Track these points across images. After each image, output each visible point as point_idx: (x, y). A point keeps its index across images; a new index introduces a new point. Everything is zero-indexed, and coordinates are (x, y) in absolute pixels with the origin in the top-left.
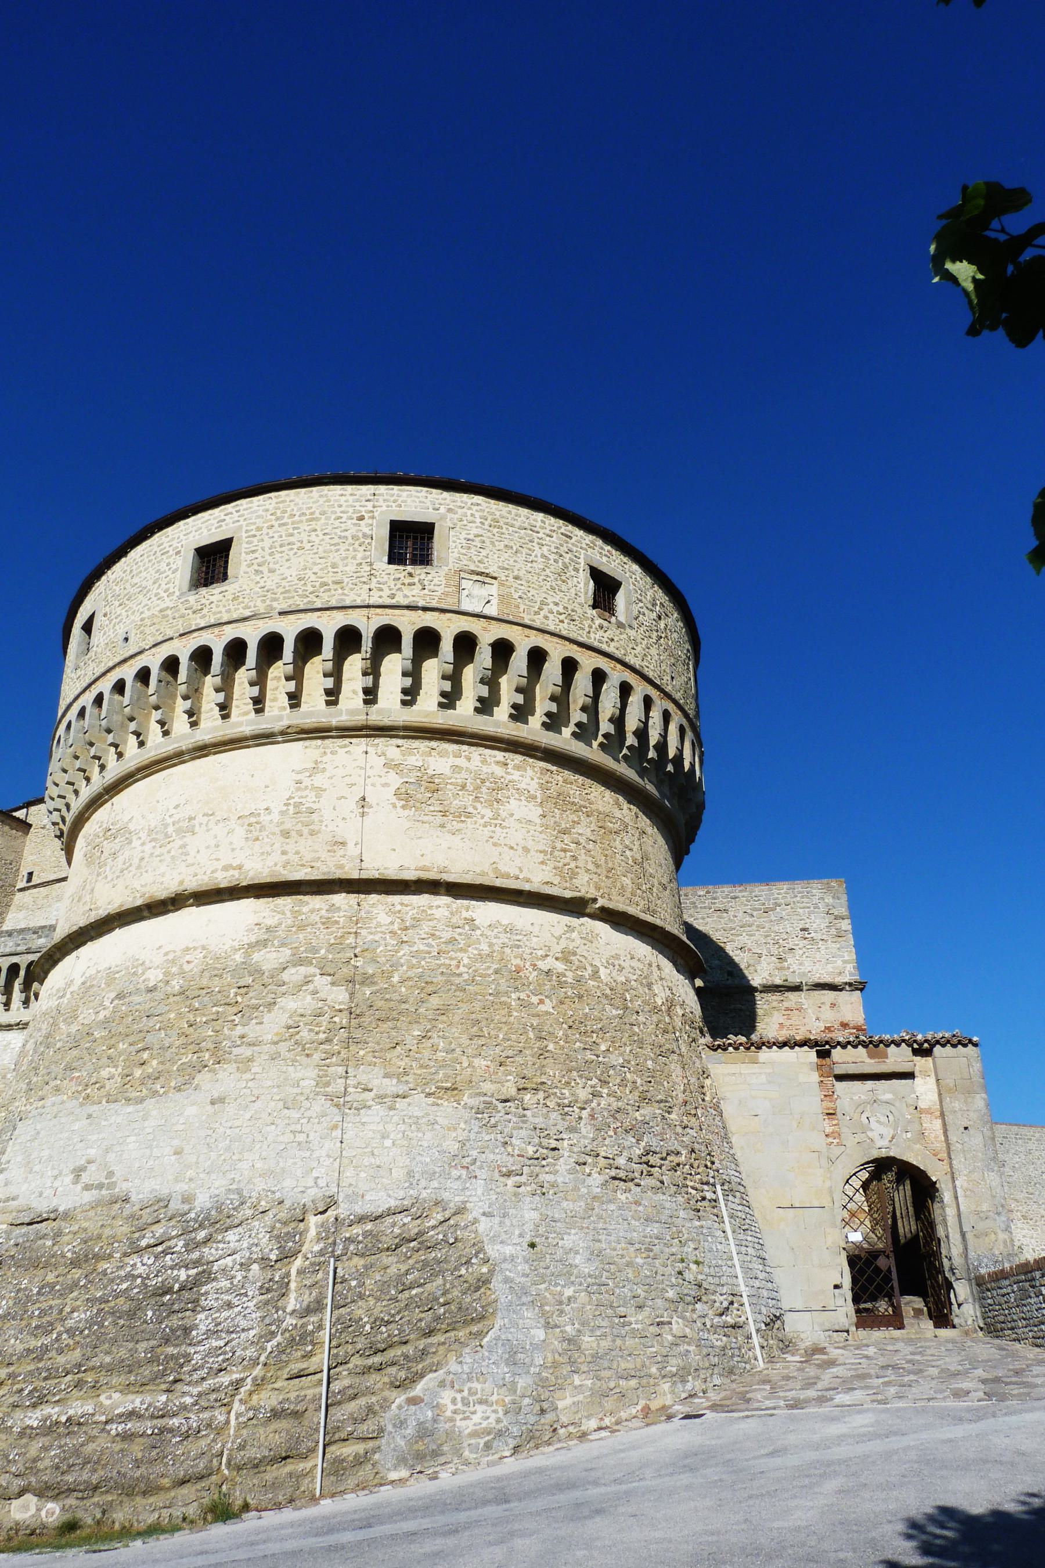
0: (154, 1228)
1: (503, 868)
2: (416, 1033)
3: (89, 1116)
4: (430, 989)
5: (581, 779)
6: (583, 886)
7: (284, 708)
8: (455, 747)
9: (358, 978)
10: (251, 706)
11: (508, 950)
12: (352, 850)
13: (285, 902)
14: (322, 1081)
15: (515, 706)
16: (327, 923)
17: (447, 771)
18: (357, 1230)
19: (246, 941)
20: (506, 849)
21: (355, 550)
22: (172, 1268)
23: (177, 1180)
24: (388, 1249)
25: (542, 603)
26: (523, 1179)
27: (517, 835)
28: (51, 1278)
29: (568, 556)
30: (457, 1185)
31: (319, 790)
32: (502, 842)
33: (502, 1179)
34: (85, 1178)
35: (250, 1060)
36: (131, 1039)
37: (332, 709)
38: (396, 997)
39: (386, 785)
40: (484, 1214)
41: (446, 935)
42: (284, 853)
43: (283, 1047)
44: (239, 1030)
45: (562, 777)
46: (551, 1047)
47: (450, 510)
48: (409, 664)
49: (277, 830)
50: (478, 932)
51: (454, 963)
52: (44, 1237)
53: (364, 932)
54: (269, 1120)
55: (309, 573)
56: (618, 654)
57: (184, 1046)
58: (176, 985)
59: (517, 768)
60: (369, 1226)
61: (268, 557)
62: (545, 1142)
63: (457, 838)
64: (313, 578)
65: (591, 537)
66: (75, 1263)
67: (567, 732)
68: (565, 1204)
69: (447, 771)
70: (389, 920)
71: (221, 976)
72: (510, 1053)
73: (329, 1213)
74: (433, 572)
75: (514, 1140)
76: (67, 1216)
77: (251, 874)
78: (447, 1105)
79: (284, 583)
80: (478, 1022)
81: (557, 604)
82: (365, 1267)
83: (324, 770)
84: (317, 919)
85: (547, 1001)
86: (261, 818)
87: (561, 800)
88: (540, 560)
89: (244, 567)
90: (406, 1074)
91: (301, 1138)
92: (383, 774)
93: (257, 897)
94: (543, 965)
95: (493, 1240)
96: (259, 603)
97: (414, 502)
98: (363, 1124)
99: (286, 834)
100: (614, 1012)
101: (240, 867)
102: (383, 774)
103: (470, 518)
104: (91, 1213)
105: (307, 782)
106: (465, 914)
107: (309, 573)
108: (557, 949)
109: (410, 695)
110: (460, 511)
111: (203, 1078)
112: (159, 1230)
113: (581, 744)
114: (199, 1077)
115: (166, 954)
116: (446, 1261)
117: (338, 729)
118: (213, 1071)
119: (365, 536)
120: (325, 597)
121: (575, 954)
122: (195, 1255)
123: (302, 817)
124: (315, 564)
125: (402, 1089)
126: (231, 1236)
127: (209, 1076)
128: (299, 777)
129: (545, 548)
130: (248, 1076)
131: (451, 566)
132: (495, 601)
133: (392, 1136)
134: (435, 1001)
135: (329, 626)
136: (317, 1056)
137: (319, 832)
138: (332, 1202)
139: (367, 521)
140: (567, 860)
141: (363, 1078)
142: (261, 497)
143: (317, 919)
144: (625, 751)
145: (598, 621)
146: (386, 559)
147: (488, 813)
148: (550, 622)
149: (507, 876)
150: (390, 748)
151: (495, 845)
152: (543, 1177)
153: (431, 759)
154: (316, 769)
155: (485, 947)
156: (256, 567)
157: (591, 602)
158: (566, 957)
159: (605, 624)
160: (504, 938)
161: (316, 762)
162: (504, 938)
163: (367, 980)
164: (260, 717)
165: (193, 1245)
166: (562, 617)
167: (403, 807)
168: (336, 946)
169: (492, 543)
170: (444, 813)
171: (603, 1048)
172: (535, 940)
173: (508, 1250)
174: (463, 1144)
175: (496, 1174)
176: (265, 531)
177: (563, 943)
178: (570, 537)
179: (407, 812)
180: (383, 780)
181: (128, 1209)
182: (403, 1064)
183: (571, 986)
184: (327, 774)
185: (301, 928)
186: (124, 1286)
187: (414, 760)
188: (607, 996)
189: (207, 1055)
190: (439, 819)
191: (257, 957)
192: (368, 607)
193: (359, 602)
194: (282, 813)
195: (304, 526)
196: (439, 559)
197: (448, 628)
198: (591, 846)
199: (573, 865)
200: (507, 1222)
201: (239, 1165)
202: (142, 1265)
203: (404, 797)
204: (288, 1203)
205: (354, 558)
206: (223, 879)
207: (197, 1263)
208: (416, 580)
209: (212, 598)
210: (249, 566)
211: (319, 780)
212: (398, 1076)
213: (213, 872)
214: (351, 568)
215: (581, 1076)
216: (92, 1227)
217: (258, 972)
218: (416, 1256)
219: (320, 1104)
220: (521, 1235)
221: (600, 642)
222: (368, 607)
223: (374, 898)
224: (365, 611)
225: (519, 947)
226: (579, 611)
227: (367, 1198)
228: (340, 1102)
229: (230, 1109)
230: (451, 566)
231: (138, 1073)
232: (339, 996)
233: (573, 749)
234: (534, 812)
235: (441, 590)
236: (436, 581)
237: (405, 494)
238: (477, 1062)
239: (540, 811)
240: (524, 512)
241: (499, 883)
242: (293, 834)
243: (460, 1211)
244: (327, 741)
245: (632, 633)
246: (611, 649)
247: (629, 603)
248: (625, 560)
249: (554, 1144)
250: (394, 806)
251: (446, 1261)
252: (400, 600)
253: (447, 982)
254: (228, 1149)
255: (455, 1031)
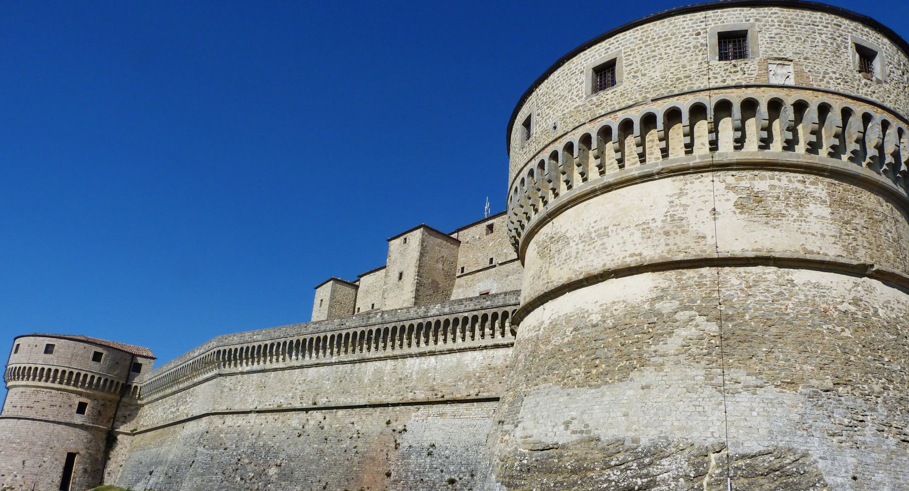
0: (617, 455)
1: (809, 248)
2: (764, 349)
3: (568, 394)
4: (770, 323)
5: (854, 188)
6: (862, 257)
7: (658, 158)
8: (770, 173)
9: (723, 317)
10: (638, 159)
11: (817, 299)
12: (710, 241)
13: (672, 274)
14: (709, 377)
15: (810, 144)
16: (700, 285)
17: (767, 189)
18: (740, 463)
19: (650, 297)
20: (810, 236)
21: (696, 55)
22: (632, 477)
23: (627, 430)
24: (762, 475)
25: (825, 73)
26: (843, 438)
27: (816, 227)
28: (560, 478)
29: (840, 39)
30: (801, 440)
31: (685, 207)
32: (807, 231)
33: (831, 438)
34: (572, 427)
35: (662, 364)
36: (587, 353)
37: (689, 156)
38: (748, 328)
39: (728, 200)
40: (820, 458)
41: (777, 290)
42: (667, 245)
43: (682, 358)
44: (653, 348)
46: (852, 358)
47: (757, 20)
48: (738, 123)
49: (661, 231)
50: (797, 288)
51: (783, 307)
52: (553, 457)
53: (723, 290)
54: (679, 398)
55: (668, 73)
56: (879, 101)
57: (620, 356)
58: (610, 322)
59: (812, 183)
60: (748, 461)
61: (640, 67)
62: (855, 417)
63: (777, 231)
64: (671, 76)
65: (854, 24)
66: (573, 472)
67: (845, 158)
68: (873, 455)
69: (767, 189)
70: (739, 282)
71: (637, 317)
72: (826, 362)
73: (722, 452)
74: (750, 63)
75: (835, 415)
76: (564, 447)
77: (648, 258)
78: (789, 393)
79: (652, 82)
80: (803, 343)
81: (834, 73)
82: (748, 484)
83: (687, 194)
84: (693, 283)
85: (847, 330)
86: (651, 225)
87: (842, 203)
88: (821, 44)
89: (625, 75)
90: (760, 373)
91: (700, 409)
92: (725, 193)
93: (653, 271)
94: (844, 307)
95: (828, 473)
96: (638, 96)
98: (738, 402)
99: (667, 233)
100: (891, 337)
101: (640, 254)
102: (725, 193)
103: (771, 23)
104: (579, 446)
105: (677, 202)
106: (787, 277)
107: (668, 73)
108: (849, 297)
109: (740, 143)
110: (764, 19)
111: (634, 374)
112: (621, 457)
113: (855, 165)
114: (632, 374)
115: (601, 305)
116: (799, 484)
117: (693, 168)
118: (640, 370)
119: (702, 45)
120: (680, 87)
121: (861, 300)
122: (645, 471)
123: (676, 223)
124: (671, 67)
125: (759, 383)
126: (665, 462)
127: (638, 373)
128: (670, 199)
129: (823, 36)
130: (663, 374)
131: (761, 57)
132: (792, 76)
133: (757, 409)
134: (774, 330)
135: (684, 104)
136: (703, 363)
137: (688, 231)
138: (723, 447)
139: (702, 35)
140: (850, 241)
141: (735, 376)
142: (631, 31)
143: (693, 283)
144: (885, 167)
145: (864, 81)
146: (717, 58)
147: (796, 214)
148: (831, 85)
149: (812, 252)
150: (729, 177)
151: (802, 233)
152: (856, 438)
153: (755, 182)
154: (681, 193)
155: (802, 297)
156: (633, 74)
157: (858, 69)
158: (856, 302)
159: (869, 82)
160: (814, 291)
161: (681, 189)
162: (814, 291)
163: (729, 318)
164: (643, 165)
165: (642, 466)
166: (839, 81)
167: (740, 213)
168: (707, 298)
169: (787, 38)
170: (767, 215)
171: (886, 359)
172: (834, 292)
173: (839, 480)
174: (802, 416)
175: (826, 435)
176: (636, 51)
177: (853, 294)
178: (840, 26)
179: (743, 216)
180: (726, 197)
181: (600, 445)
182: (758, 368)
183: (861, 320)
184: (689, 196)
185: (684, 288)
186: (605, 485)
187: (744, 184)
188: (885, 327)
189: (635, 362)
190: (764, 219)
191: (657, 306)
192: (709, 89)
193: (702, 87)
194: (663, 221)
195: (662, 44)
196: (753, 53)
197: (763, 97)
198: (865, 231)
199: (854, 244)
200: (836, 463)
201: (664, 423)
202: (614, 475)
203: (741, 206)
204: (696, 446)
205: (696, 60)
206: (632, 262)
207: (647, 476)
208: (739, 69)
209: (607, 97)
210: (629, 74)
211: (684, 200)
212: (756, 375)
213: (624, 258)
214: (695, 67)
215: (874, 377)
216: (581, 453)
217: (659, 314)
218: (780, 480)
219: (709, 391)
220: (846, 472)
221: (866, 94)
222: (709, 89)
223: (727, 269)
224: (708, 93)
225: (824, 296)
226: (850, 75)
227: (745, 445)
228: (721, 389)
229: (654, 392)
230: (761, 57)
231: (594, 371)
232: (713, 328)
233: (850, 168)
234: (826, 211)
235: (755, 73)
236: (752, 68)
237: (725, 14)
238: (805, 367)
239: (830, 210)
240: (807, 13)
241: (808, 257)
242: (672, 233)
243: (805, 455)
244: (687, 176)
245: (887, 86)
246: (874, 98)
247: (883, 66)
248: (879, 36)
249: (861, 418)
250: (735, 213)
251: (799, 484)
252: (729, 82)
253: (780, 319)
254: (656, 414)
255: (789, 348)
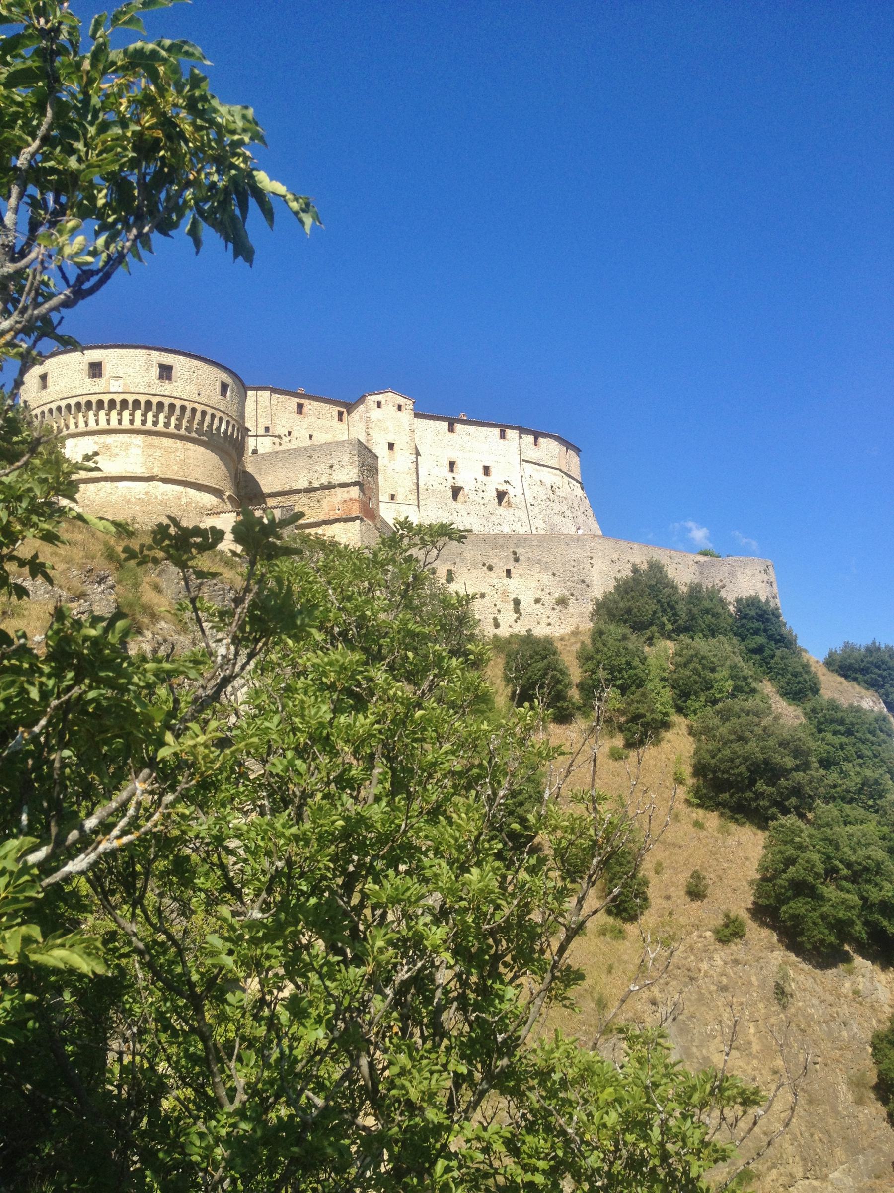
6: (156, 471)
45: (150, 439)
87: (151, 446)
97: (94, 355)
150: (96, 438)
163: (88, 505)
234: (139, 451)
246: (166, 393)
